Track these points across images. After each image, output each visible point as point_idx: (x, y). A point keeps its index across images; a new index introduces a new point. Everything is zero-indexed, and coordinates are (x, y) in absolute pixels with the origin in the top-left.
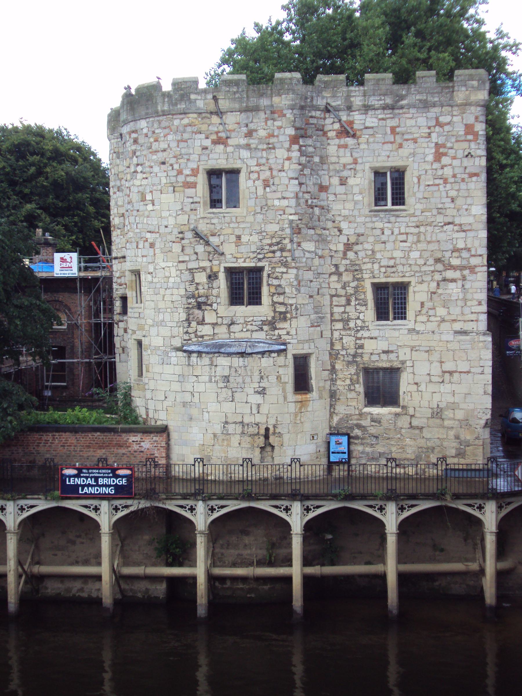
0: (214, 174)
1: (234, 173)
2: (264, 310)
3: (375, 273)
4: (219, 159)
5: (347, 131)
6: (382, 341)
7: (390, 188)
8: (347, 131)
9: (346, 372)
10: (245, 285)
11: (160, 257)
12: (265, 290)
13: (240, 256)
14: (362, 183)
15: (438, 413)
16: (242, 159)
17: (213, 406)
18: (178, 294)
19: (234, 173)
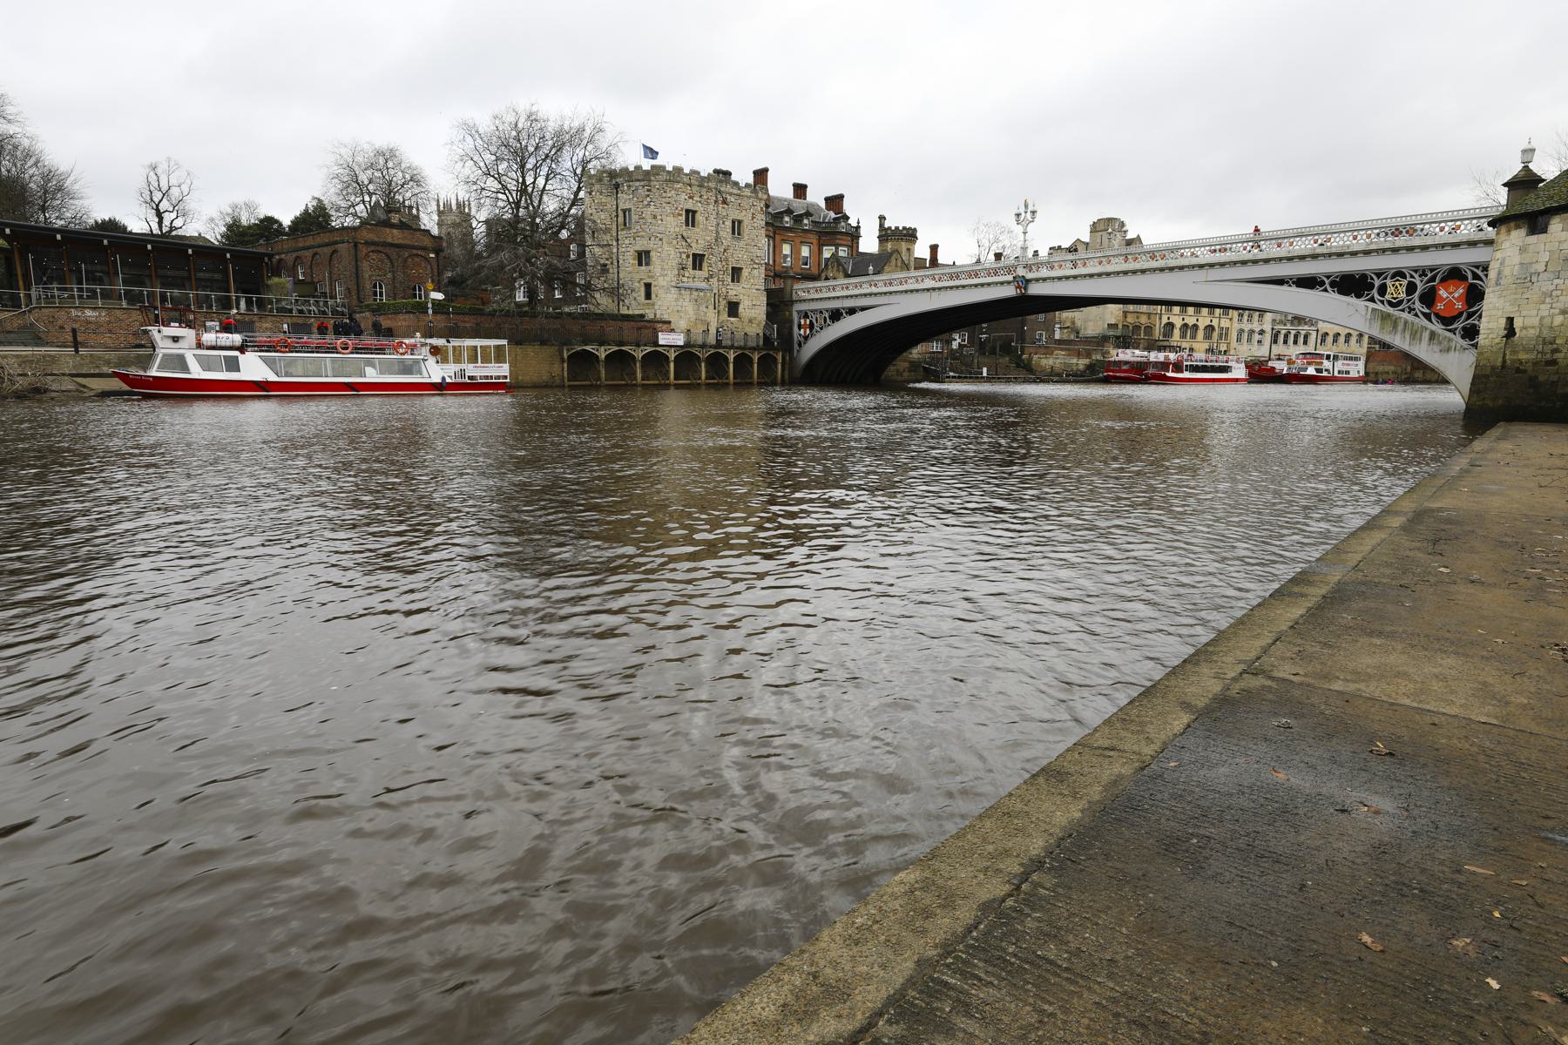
0: (687, 211)
1: (694, 212)
2: (704, 273)
3: (733, 263)
4: (690, 205)
5: (724, 202)
6: (734, 291)
7: (737, 227)
8: (724, 202)
9: (723, 303)
10: (698, 261)
11: (666, 247)
12: (705, 265)
13: (697, 249)
14: (729, 224)
15: (750, 321)
16: (699, 207)
17: (691, 312)
18: (675, 263)
19: (694, 212)
